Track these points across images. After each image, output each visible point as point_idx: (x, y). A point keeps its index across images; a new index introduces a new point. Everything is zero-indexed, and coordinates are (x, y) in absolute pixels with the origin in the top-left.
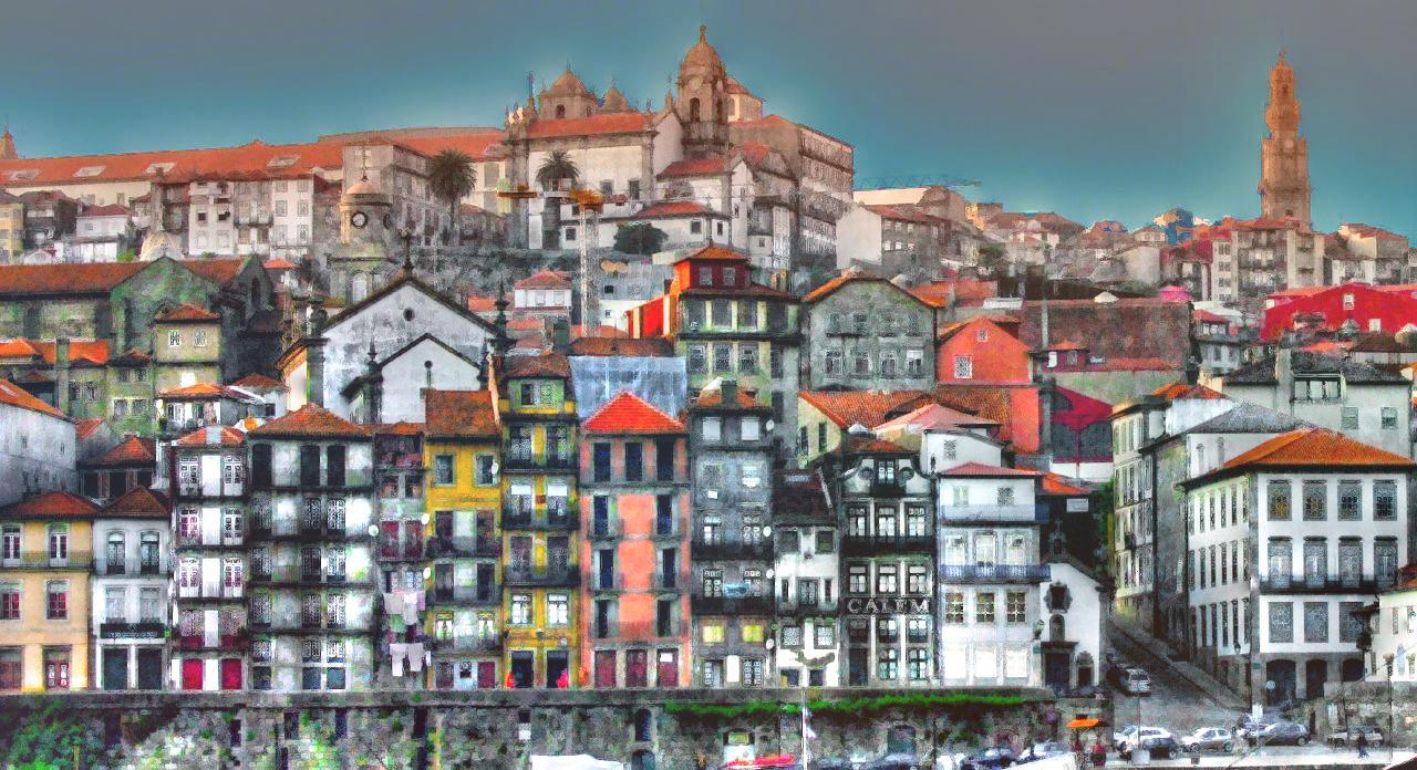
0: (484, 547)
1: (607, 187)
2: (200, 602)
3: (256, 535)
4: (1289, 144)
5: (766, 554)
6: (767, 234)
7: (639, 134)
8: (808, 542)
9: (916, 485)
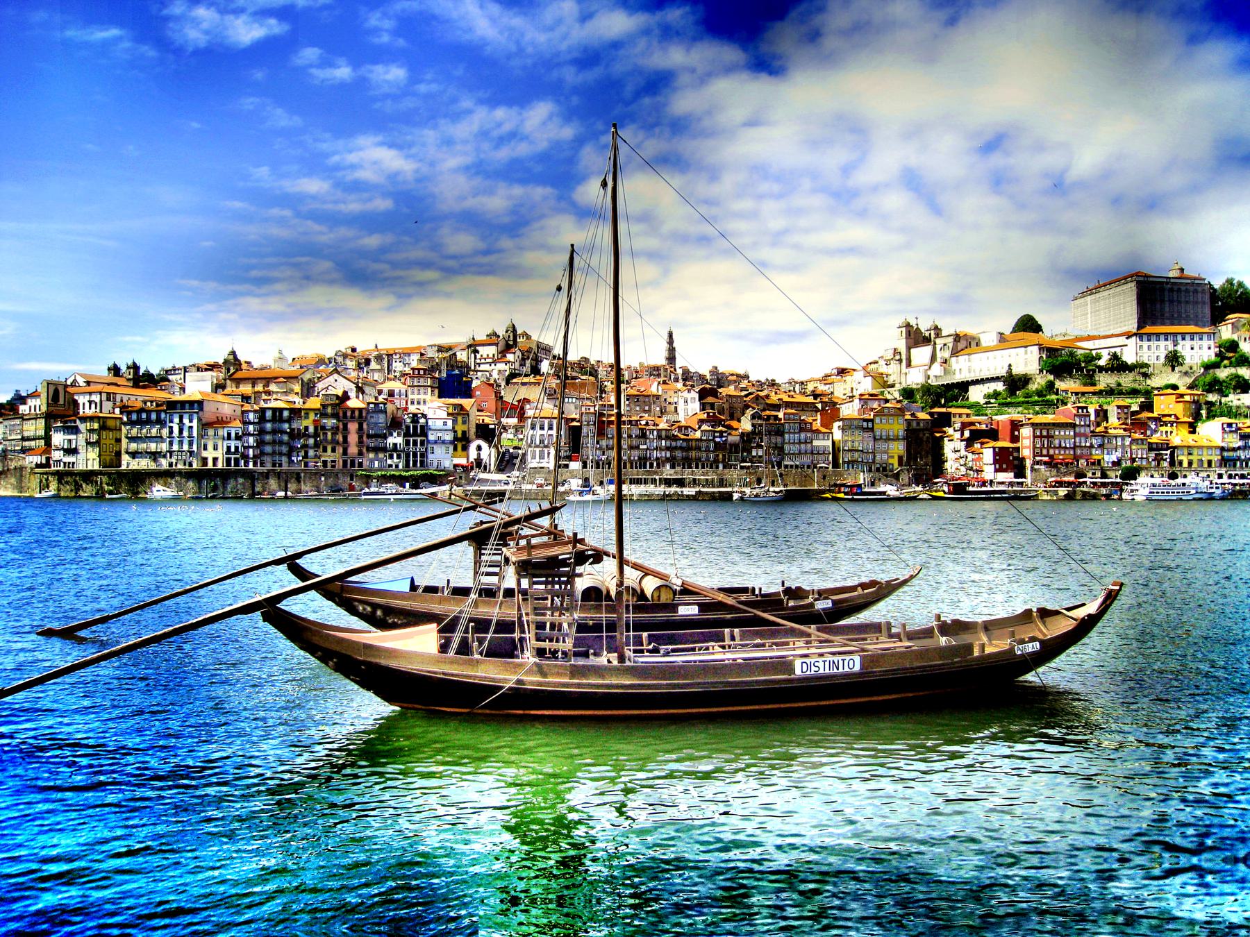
0: (316, 435)
2: (249, 447)
3: (262, 432)
5: (385, 437)
8: (395, 434)
9: (422, 421)
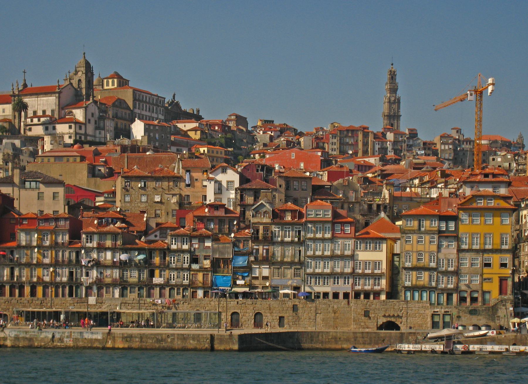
1: (44, 112)
4: (393, 99)
6: (103, 130)
7: (55, 93)
